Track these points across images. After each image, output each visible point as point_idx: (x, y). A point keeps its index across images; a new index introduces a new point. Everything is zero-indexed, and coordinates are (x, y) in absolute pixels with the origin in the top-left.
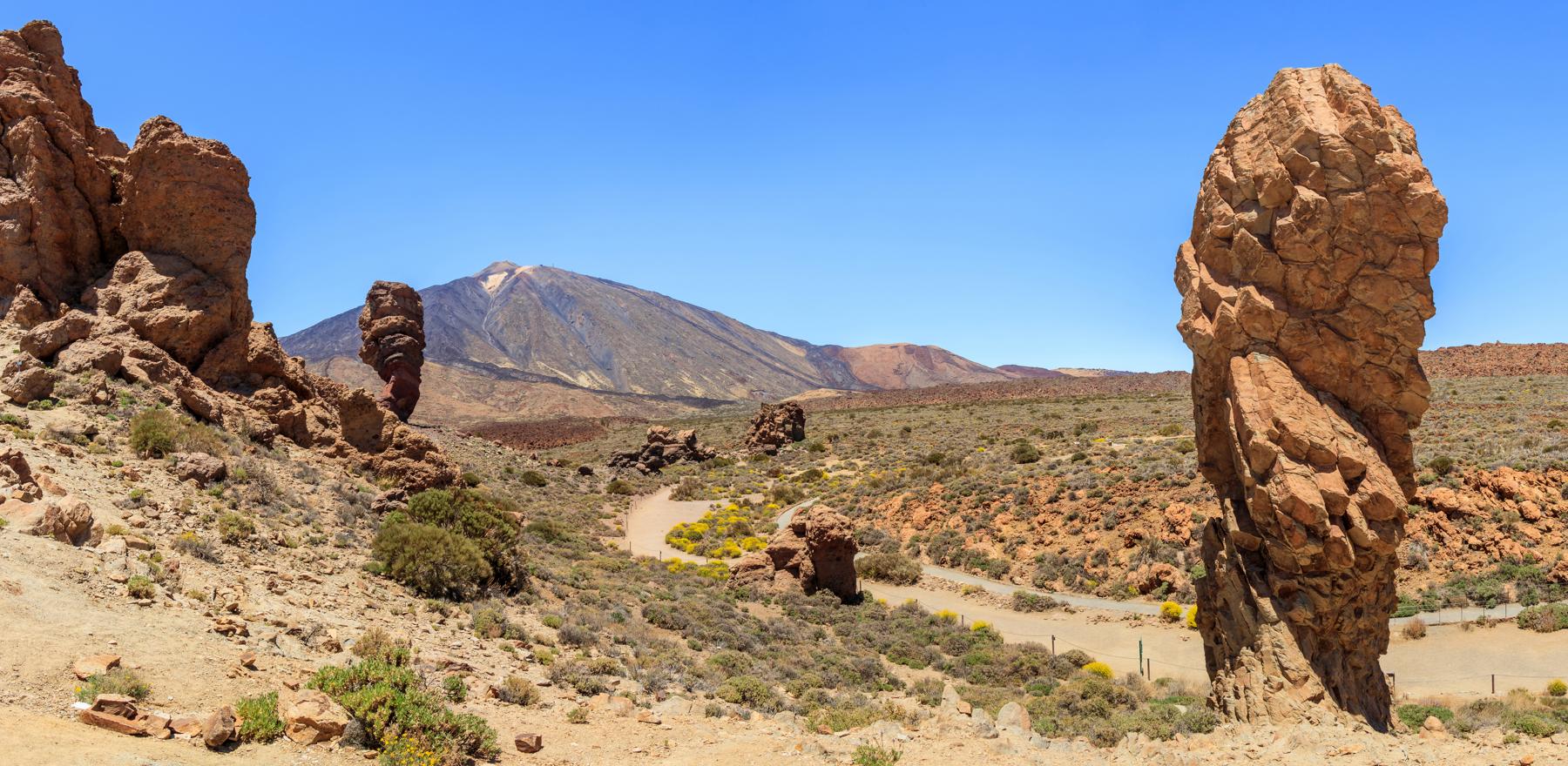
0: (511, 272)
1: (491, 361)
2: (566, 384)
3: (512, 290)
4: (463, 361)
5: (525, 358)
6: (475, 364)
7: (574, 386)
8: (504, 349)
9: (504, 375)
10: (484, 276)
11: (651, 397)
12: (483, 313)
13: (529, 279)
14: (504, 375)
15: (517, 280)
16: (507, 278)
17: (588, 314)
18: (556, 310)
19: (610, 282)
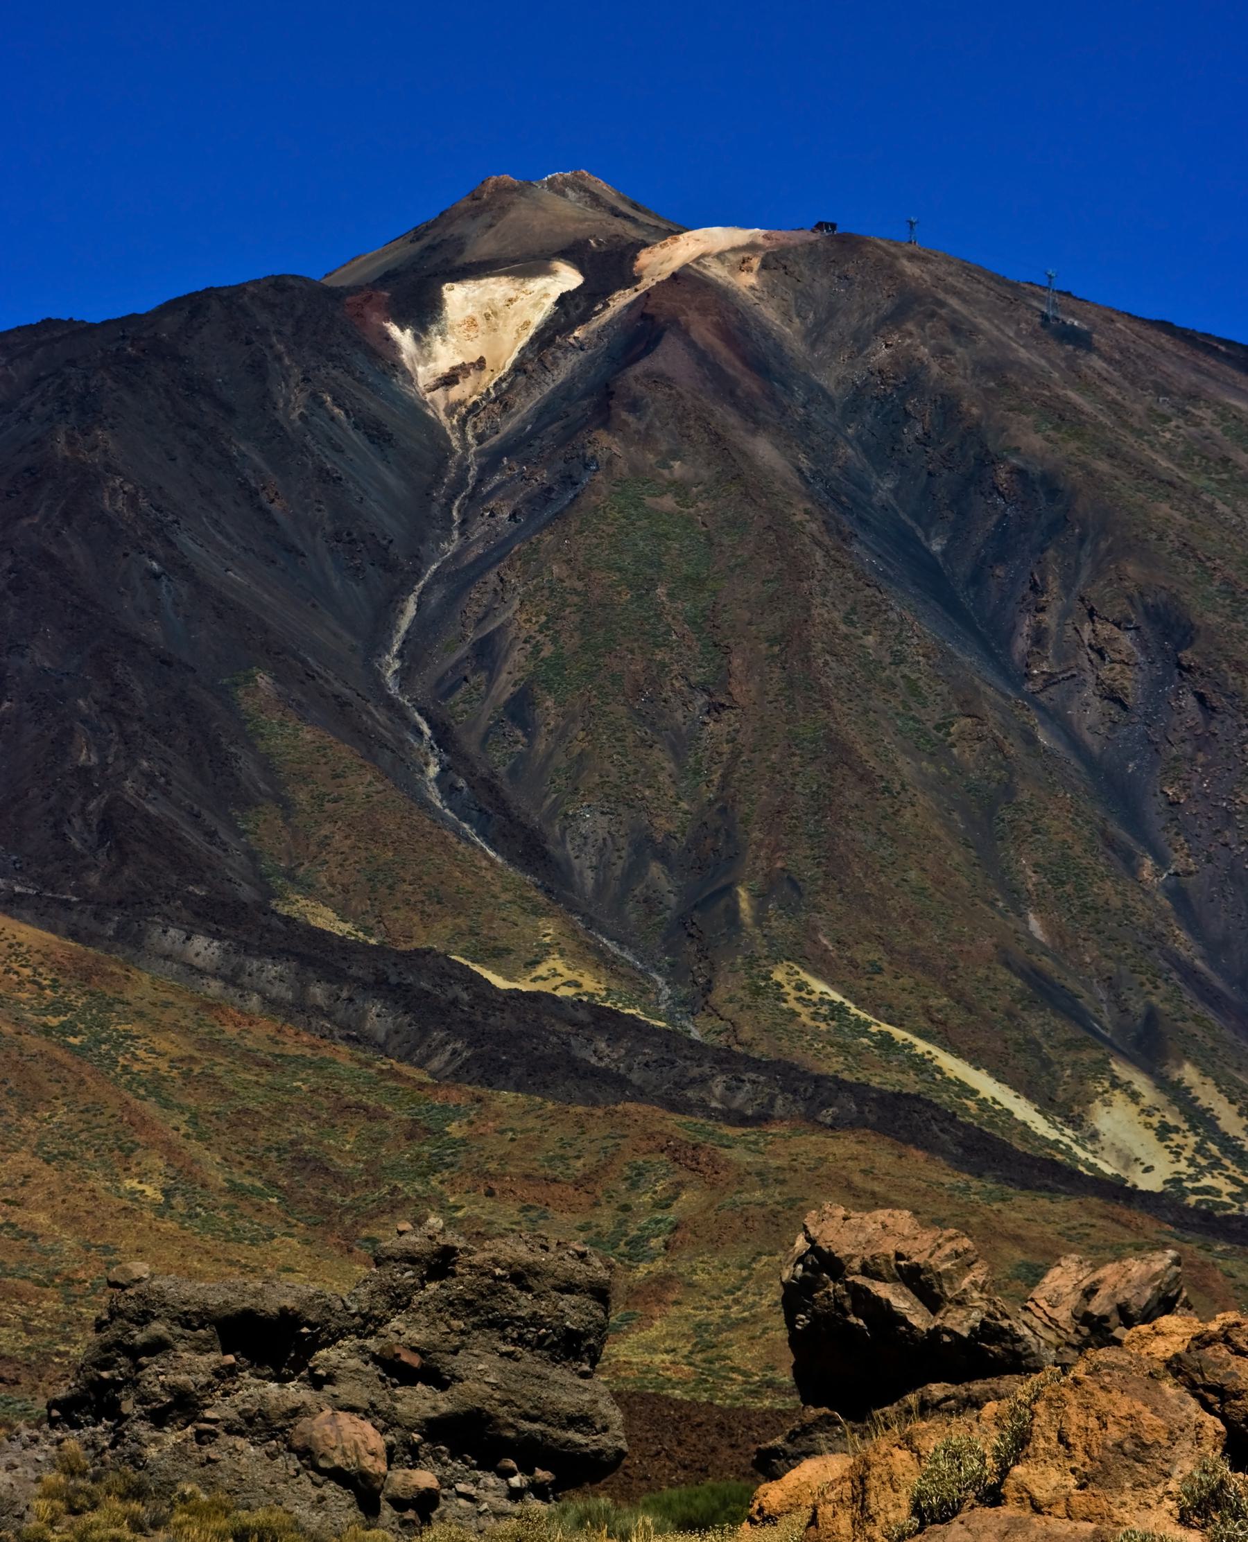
0: (607, 266)
1: (432, 937)
2: (988, 1152)
4: (218, 915)
5: (695, 934)
6: (313, 952)
7: (1050, 1174)
8: (531, 850)
9: (522, 1048)
14: (522, 1048)
15: (644, 331)
17: (1168, 629)
18: (931, 580)
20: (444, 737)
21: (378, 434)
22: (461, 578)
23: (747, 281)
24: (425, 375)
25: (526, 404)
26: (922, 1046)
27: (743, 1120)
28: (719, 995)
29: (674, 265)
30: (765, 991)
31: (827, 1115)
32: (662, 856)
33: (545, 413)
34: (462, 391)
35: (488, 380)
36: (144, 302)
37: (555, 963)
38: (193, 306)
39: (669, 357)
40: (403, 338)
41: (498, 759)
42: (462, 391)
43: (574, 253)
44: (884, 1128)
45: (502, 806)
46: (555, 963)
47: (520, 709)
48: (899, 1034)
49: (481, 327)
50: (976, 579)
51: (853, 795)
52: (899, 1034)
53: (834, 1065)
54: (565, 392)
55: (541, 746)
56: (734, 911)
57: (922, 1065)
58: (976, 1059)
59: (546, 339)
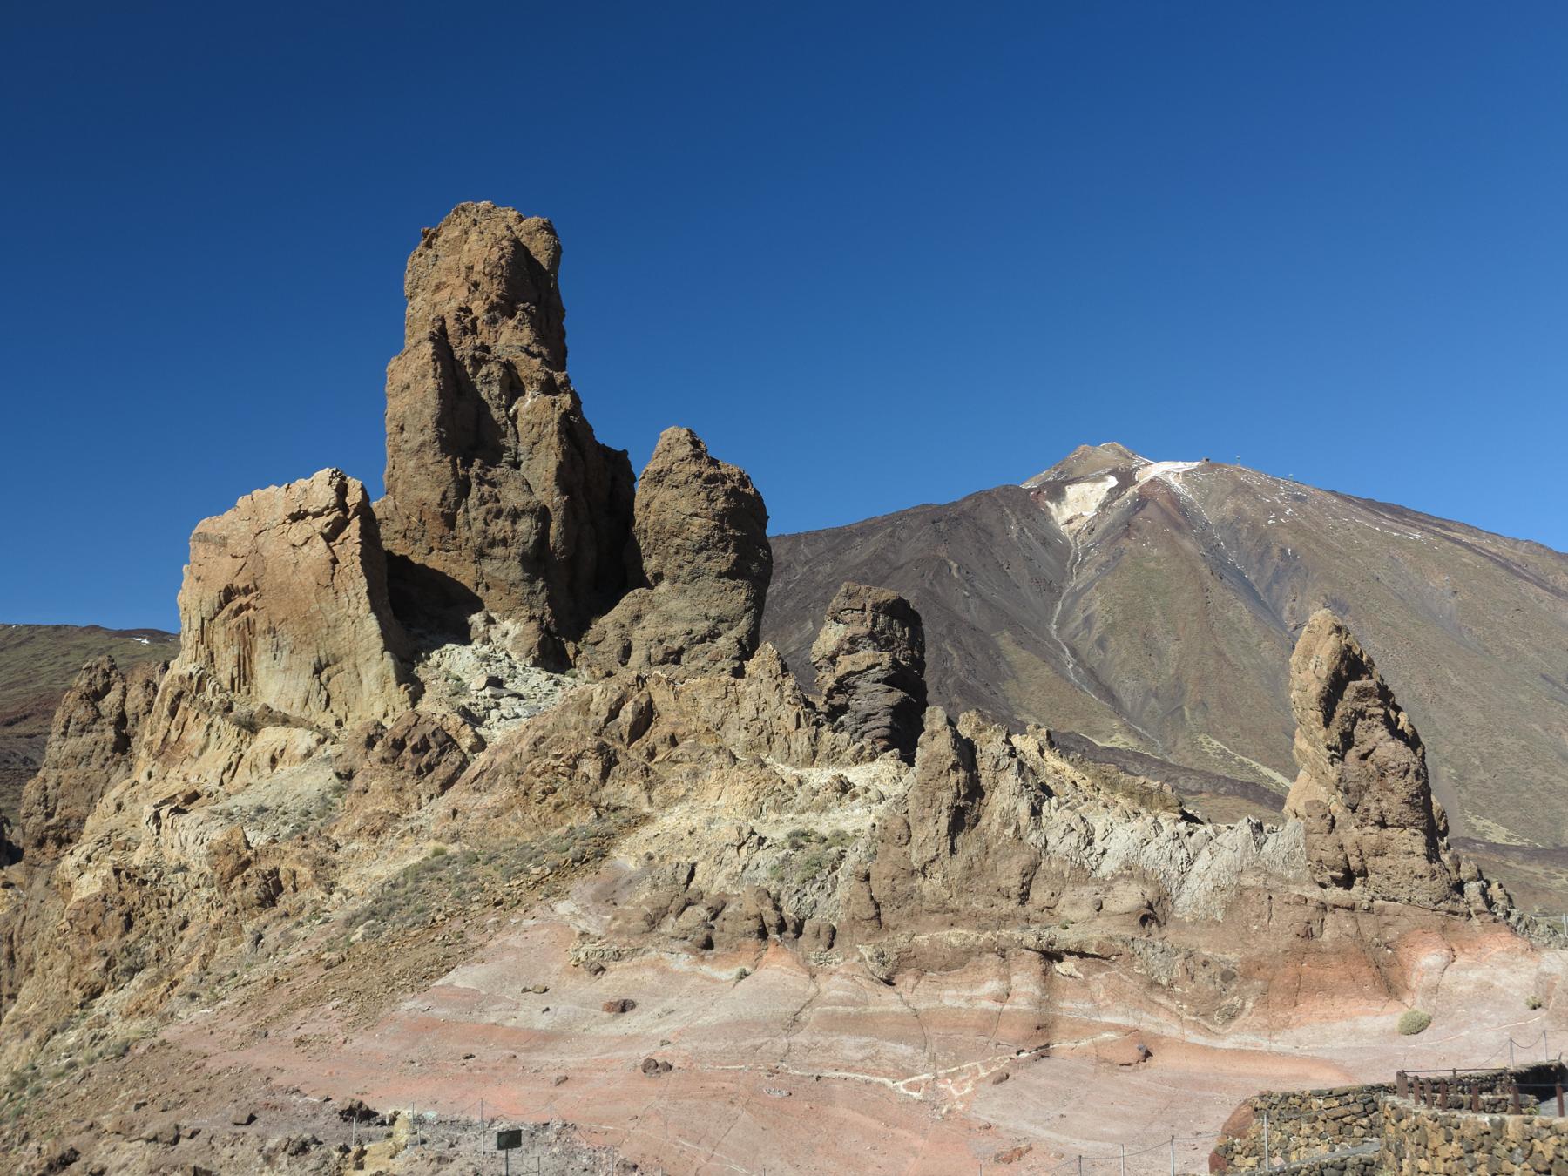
0: (1126, 478)
3: (1126, 527)
8: (1109, 694)
10: (1056, 491)
11: (1532, 854)
12: (1049, 588)
13: (1174, 498)
15: (1141, 502)
16: (1114, 493)
19: (1399, 512)
20: (1074, 653)
21: (1045, 542)
22: (1076, 595)
23: (1176, 483)
24: (1061, 520)
25: (1098, 530)
26: (1255, 764)
27: (1192, 793)
28: (1180, 745)
29: (1151, 476)
30: (1195, 744)
31: (1222, 790)
32: (1156, 696)
33: (1106, 532)
34: (1075, 525)
35: (1084, 520)
36: (957, 499)
37: (1118, 735)
38: (976, 497)
39: (1150, 510)
40: (1052, 506)
41: (1094, 661)
42: (1075, 525)
43: (1114, 472)
44: (1244, 796)
45: (1097, 679)
46: (1118, 735)
47: (1101, 643)
48: (1246, 760)
49: (1081, 504)
50: (1268, 589)
51: (1227, 671)
52: (1246, 760)
53: (1221, 771)
54: (1113, 525)
55: (1109, 656)
56: (1183, 716)
57: (1254, 771)
58: (1274, 767)
59: (1104, 506)
